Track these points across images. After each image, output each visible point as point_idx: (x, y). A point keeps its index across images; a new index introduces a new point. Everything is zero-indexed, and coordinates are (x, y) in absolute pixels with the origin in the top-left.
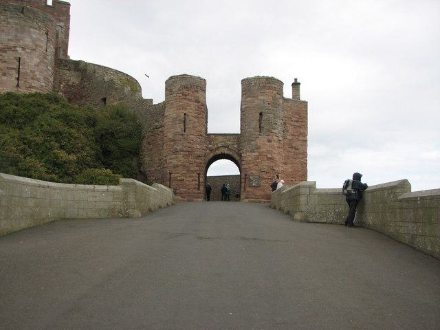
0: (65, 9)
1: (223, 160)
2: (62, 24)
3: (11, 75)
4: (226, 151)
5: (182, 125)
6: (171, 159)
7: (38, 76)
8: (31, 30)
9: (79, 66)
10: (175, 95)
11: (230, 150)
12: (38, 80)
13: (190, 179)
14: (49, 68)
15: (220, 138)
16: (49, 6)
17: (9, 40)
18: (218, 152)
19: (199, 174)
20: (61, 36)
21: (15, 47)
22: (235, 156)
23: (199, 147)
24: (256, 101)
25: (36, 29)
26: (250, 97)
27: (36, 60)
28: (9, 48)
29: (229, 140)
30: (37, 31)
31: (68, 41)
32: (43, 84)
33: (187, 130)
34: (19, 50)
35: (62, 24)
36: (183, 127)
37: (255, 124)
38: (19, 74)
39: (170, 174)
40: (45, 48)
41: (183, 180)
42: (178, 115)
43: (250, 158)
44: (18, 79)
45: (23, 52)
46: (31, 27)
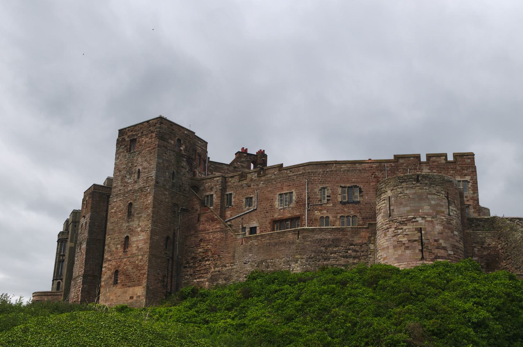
0: (469, 161)
2: (468, 178)
3: (414, 248)
7: (444, 245)
8: (429, 196)
9: (493, 224)
12: (444, 248)
14: (456, 233)
16: (450, 162)
17: (408, 212)
20: (468, 193)
21: (414, 218)
25: (434, 194)
27: (439, 228)
28: (409, 220)
30: (436, 197)
31: (478, 195)
32: (452, 253)
34: (419, 219)
35: (468, 178)
38: (422, 245)
40: (447, 212)
44: (422, 251)
45: (423, 221)
46: (428, 194)
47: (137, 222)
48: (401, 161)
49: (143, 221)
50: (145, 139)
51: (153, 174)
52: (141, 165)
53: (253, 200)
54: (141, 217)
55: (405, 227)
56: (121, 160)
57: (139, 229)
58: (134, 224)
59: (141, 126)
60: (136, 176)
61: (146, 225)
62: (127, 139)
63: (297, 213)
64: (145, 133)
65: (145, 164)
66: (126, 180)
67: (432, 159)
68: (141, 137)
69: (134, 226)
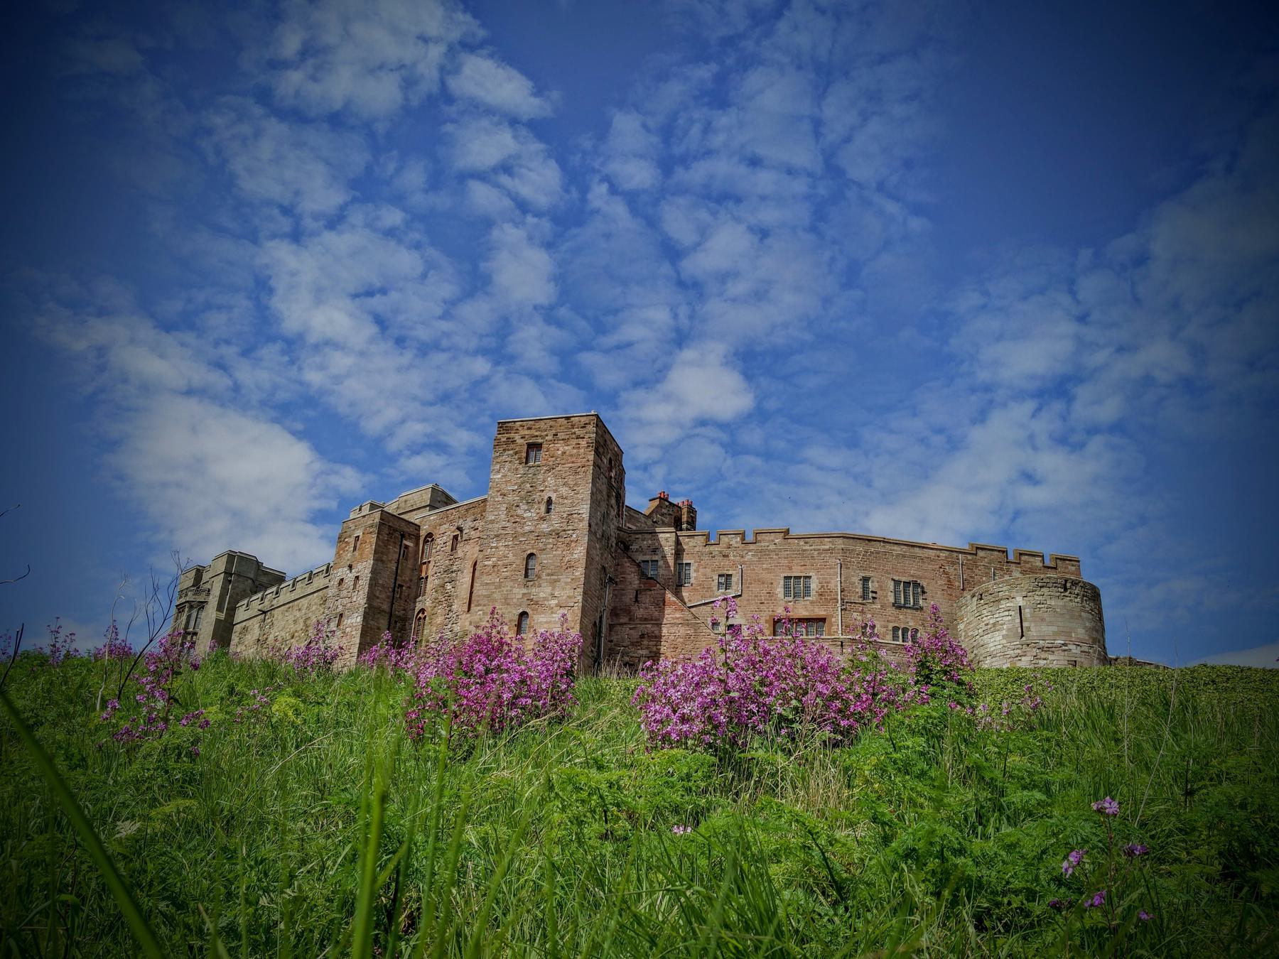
21: (1065, 645)
47: (549, 590)
48: (981, 554)
49: (564, 589)
50: (561, 448)
51: (585, 509)
52: (555, 491)
53: (734, 579)
54: (559, 580)
55: (1051, 657)
56: (504, 476)
57: (554, 602)
58: (542, 592)
59: (552, 423)
60: (543, 508)
61: (569, 597)
62: (520, 441)
63: (820, 612)
64: (561, 436)
65: (564, 491)
66: (519, 512)
67: (1024, 558)
68: (553, 441)
69: (542, 595)
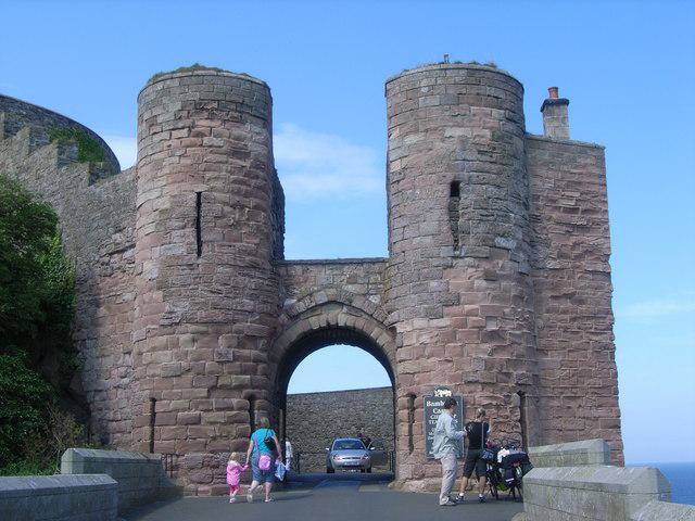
1: (343, 346)
4: (342, 318)
5: (190, 231)
6: (154, 349)
10: (165, 135)
11: (355, 311)
13: (220, 416)
15: (324, 275)
18: (316, 322)
19: (251, 398)
22: (375, 333)
23: (249, 304)
24: (438, 144)
26: (416, 131)
29: (352, 280)
33: (205, 248)
36: (193, 239)
37: (436, 219)
39: (154, 400)
41: (198, 421)
42: (177, 201)
43: (425, 338)
